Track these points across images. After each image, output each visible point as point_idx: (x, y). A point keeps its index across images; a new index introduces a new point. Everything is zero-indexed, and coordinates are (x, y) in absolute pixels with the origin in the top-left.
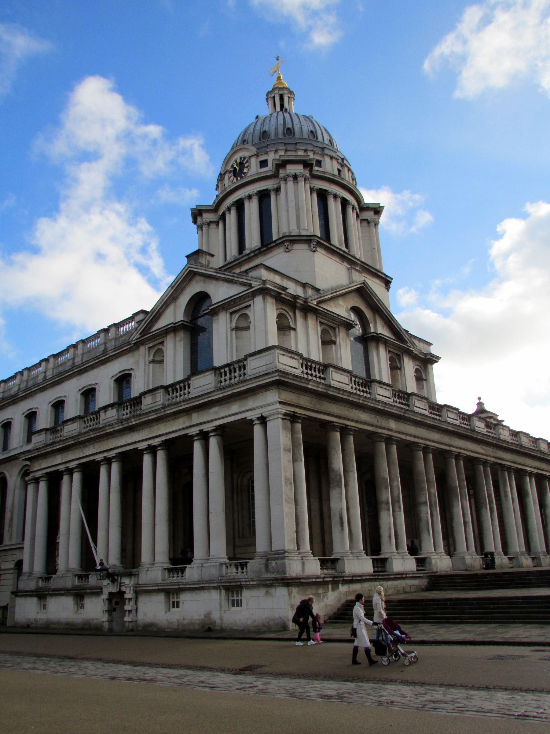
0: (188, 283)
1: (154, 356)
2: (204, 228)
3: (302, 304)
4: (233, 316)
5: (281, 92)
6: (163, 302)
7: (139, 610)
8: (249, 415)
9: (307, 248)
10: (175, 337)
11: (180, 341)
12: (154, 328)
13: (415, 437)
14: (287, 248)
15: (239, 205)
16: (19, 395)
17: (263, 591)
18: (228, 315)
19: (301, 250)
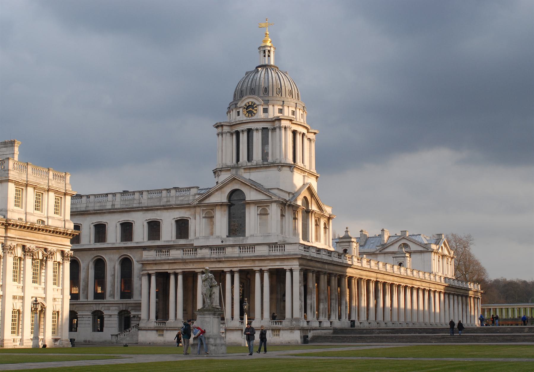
0: (231, 182)
1: (205, 215)
2: (224, 136)
3: (289, 204)
4: (259, 208)
5: (269, 49)
6: (215, 189)
7: (226, 337)
8: (285, 267)
9: (289, 170)
10: (221, 208)
11: (225, 211)
12: (207, 201)
13: (333, 271)
14: (280, 169)
15: (249, 131)
16: (90, 211)
17: (290, 331)
18: (256, 207)
19: (286, 170)
